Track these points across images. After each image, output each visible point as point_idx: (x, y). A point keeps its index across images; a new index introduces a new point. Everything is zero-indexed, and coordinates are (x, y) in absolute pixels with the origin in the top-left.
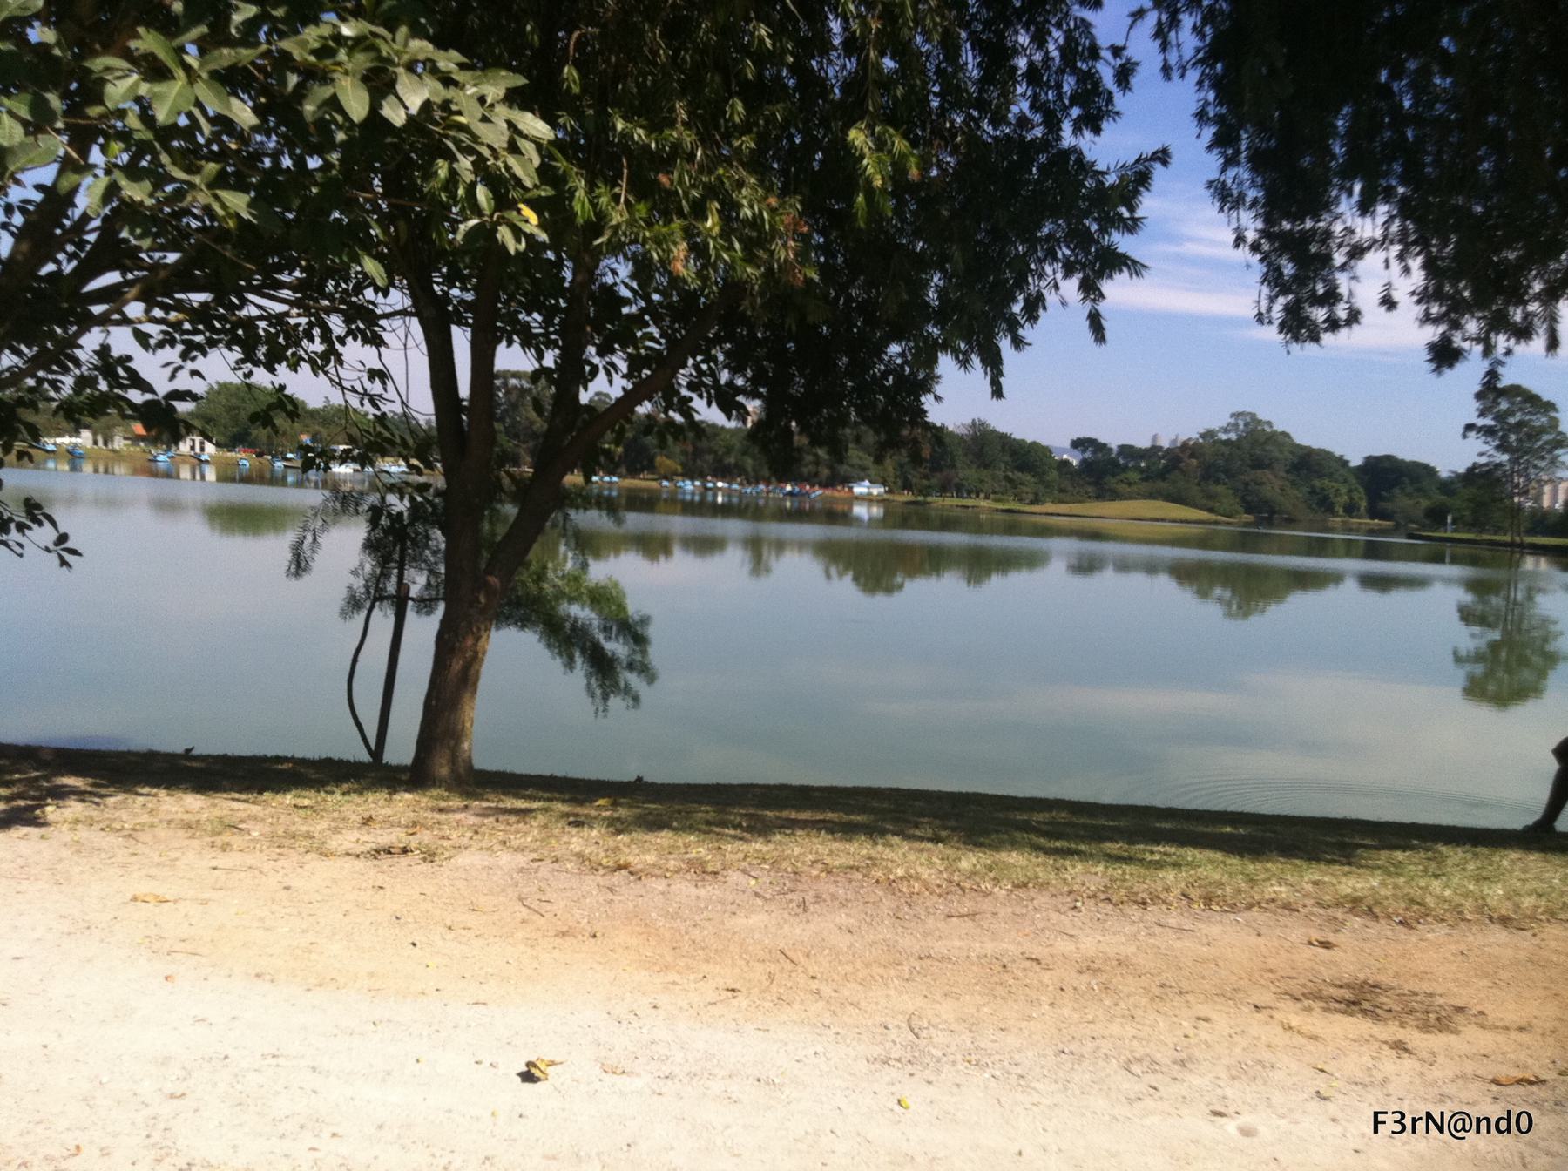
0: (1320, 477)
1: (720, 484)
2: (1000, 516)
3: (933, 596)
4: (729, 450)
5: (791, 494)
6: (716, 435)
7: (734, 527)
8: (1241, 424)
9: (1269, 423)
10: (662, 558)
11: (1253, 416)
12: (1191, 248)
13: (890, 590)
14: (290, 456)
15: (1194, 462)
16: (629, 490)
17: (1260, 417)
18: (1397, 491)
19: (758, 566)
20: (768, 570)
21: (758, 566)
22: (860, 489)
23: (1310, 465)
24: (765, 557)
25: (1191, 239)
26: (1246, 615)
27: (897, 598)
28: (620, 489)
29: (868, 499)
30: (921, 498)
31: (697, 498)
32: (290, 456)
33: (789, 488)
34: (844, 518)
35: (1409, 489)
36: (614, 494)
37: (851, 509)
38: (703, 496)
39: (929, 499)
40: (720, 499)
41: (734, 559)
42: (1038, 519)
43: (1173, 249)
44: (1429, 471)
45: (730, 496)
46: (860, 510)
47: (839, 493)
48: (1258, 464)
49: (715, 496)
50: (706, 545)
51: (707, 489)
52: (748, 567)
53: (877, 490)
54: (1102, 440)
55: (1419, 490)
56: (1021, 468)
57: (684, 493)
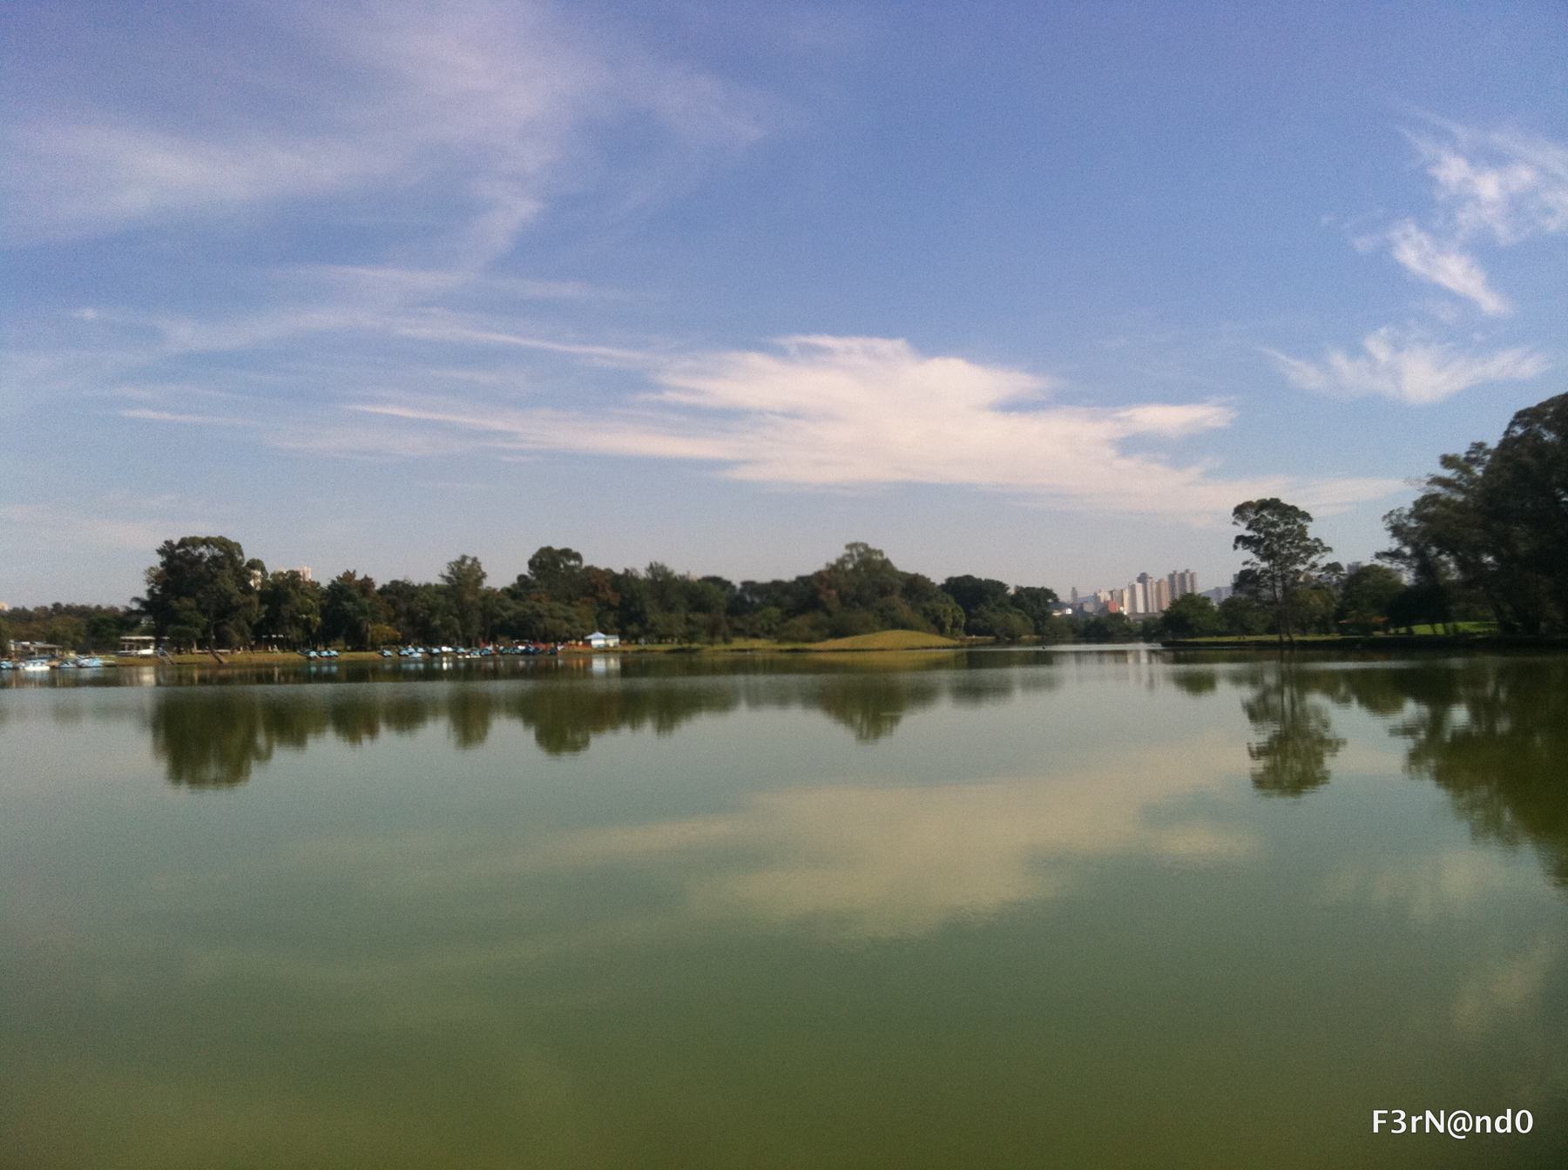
0: (928, 599)
1: (445, 649)
2: (785, 656)
3: (621, 749)
4: (433, 610)
6: (413, 596)
9: (881, 552)
11: (865, 546)
12: (670, 397)
13: (576, 747)
16: (349, 663)
17: (871, 546)
18: (982, 608)
23: (915, 586)
26: (877, 735)
28: (339, 664)
29: (605, 651)
30: (686, 645)
31: (421, 666)
34: (586, 671)
35: (992, 605)
36: (334, 669)
39: (695, 646)
43: (655, 397)
44: (1001, 587)
46: (598, 665)
48: (884, 592)
53: (613, 641)
54: (726, 577)
55: (1000, 605)
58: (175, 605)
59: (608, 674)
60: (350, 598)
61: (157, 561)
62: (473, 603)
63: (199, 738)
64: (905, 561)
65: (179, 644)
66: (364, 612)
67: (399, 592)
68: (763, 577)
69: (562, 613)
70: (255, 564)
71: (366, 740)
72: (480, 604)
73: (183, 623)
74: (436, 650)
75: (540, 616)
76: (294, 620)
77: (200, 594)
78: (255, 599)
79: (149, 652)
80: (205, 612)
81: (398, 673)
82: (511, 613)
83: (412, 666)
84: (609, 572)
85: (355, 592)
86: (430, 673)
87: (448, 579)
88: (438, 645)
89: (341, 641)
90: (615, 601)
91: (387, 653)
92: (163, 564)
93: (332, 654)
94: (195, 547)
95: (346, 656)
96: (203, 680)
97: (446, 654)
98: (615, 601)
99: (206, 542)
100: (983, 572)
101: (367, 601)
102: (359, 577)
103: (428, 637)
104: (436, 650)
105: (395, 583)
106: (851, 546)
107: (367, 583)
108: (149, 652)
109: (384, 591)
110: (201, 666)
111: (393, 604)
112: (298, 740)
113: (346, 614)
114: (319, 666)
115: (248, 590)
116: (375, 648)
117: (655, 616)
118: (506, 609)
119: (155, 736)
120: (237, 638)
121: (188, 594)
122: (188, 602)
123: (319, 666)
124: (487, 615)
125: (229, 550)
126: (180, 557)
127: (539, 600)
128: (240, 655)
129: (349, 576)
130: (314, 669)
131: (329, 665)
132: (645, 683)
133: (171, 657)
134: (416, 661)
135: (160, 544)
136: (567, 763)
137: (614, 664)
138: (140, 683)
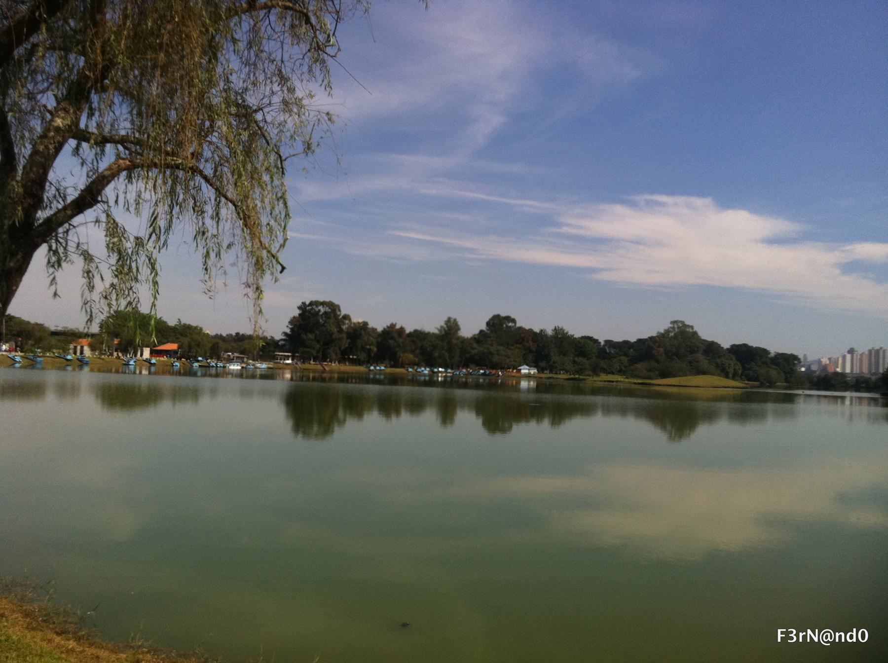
0: (720, 357)
1: (440, 369)
4: (434, 347)
5: (482, 374)
6: (425, 338)
8: (676, 326)
9: (692, 327)
11: (682, 322)
12: (565, 230)
15: (661, 350)
17: (687, 323)
23: (712, 348)
25: (568, 225)
28: (385, 374)
29: (528, 377)
31: (427, 378)
34: (516, 388)
41: (430, 417)
42: (693, 391)
44: (765, 352)
46: (524, 384)
49: (438, 377)
50: (416, 406)
51: (434, 372)
53: (533, 371)
54: (596, 337)
55: (764, 363)
56: (578, 355)
58: (304, 336)
59: (529, 390)
60: (393, 338)
61: (297, 313)
63: (310, 410)
64: (706, 333)
65: (304, 359)
66: (399, 346)
67: (418, 336)
68: (618, 338)
69: (504, 353)
70: (346, 317)
71: (394, 418)
75: (491, 354)
76: (363, 348)
77: (317, 332)
78: (344, 335)
79: (289, 361)
80: (318, 342)
81: (414, 381)
82: (476, 351)
84: (531, 330)
85: (395, 335)
86: (431, 383)
89: (387, 362)
90: (534, 348)
91: (410, 370)
92: (300, 315)
94: (317, 306)
95: (389, 370)
96: (314, 379)
97: (441, 372)
98: (534, 348)
99: (323, 304)
101: (401, 340)
102: (398, 327)
103: (431, 362)
105: (416, 331)
106: (673, 322)
107: (402, 330)
108: (289, 361)
109: (410, 335)
110: (314, 371)
111: (414, 342)
113: (390, 347)
114: (375, 374)
115: (341, 331)
116: (402, 366)
117: (556, 358)
118: (473, 349)
120: (334, 357)
122: (311, 336)
125: (333, 308)
126: (309, 311)
127: (492, 345)
128: (335, 366)
129: (393, 326)
130: (372, 376)
131: (380, 374)
133: (300, 365)
134: (425, 375)
135: (299, 304)
137: (533, 384)
138: (283, 378)
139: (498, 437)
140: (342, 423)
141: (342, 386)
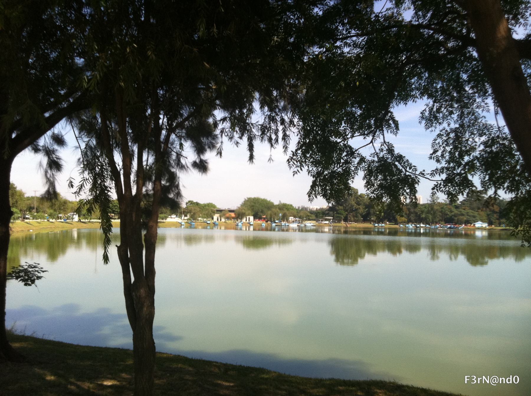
1: (422, 225)
4: (422, 212)
5: (450, 228)
7: (423, 240)
10: (398, 254)
14: (277, 221)
19: (434, 256)
20: (438, 258)
21: (434, 256)
22: (478, 224)
24: (436, 251)
27: (485, 267)
29: (481, 229)
31: (413, 231)
32: (277, 221)
33: (449, 226)
34: (473, 237)
36: (383, 230)
37: (474, 233)
38: (416, 230)
40: (422, 231)
41: (424, 254)
45: (426, 230)
46: (478, 234)
47: (469, 226)
49: (420, 230)
50: (413, 248)
51: (417, 227)
52: (430, 256)
53: (485, 225)
57: (409, 229)
59: (483, 238)
62: (437, 210)
69: (472, 214)
72: (440, 210)
73: (339, 214)
74: (418, 226)
75: (463, 215)
82: (453, 213)
83: (410, 231)
86: (417, 234)
87: (445, 201)
88: (419, 223)
91: (401, 226)
93: (386, 225)
97: (422, 227)
100: (262, 195)
103: (419, 220)
104: (418, 226)
112: (375, 253)
114: (378, 229)
118: (451, 212)
119: (332, 247)
121: (341, 205)
122: (341, 207)
123: (378, 229)
124: (444, 214)
127: (464, 209)
128: (354, 224)
131: (382, 229)
132: (497, 243)
136: (478, 269)
137: (485, 233)
139: (479, 268)
140: (362, 257)
141: (366, 237)
